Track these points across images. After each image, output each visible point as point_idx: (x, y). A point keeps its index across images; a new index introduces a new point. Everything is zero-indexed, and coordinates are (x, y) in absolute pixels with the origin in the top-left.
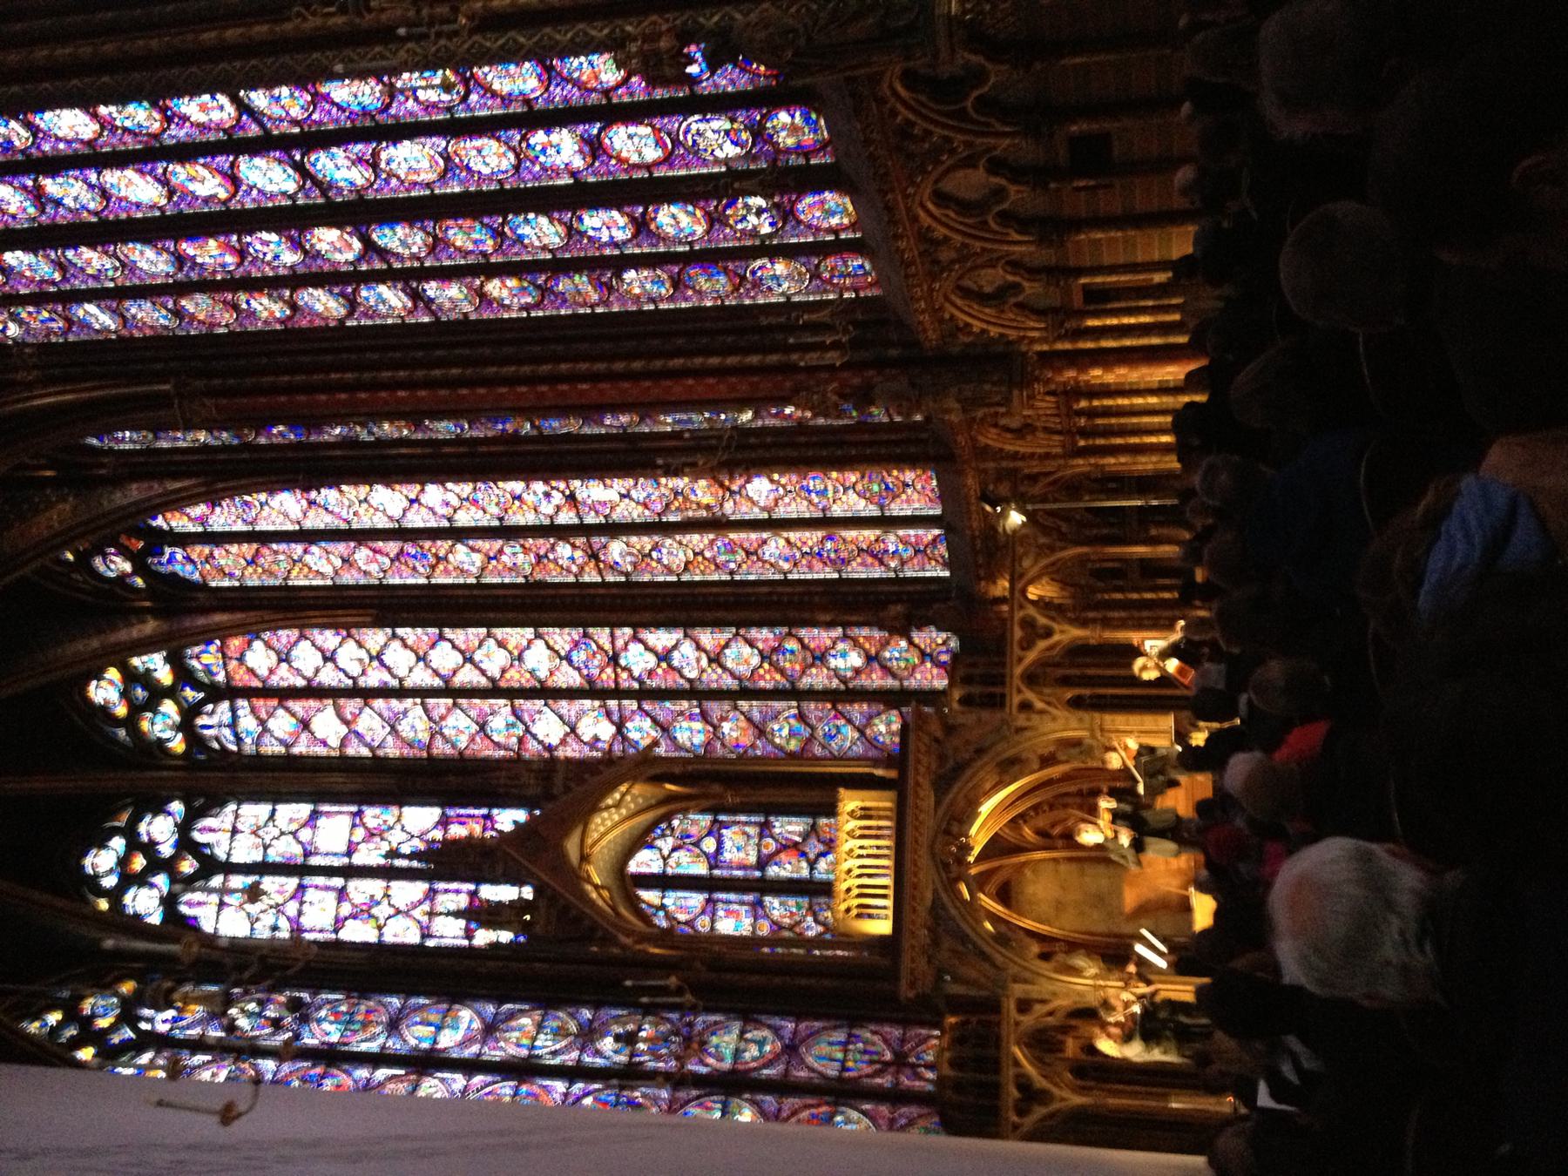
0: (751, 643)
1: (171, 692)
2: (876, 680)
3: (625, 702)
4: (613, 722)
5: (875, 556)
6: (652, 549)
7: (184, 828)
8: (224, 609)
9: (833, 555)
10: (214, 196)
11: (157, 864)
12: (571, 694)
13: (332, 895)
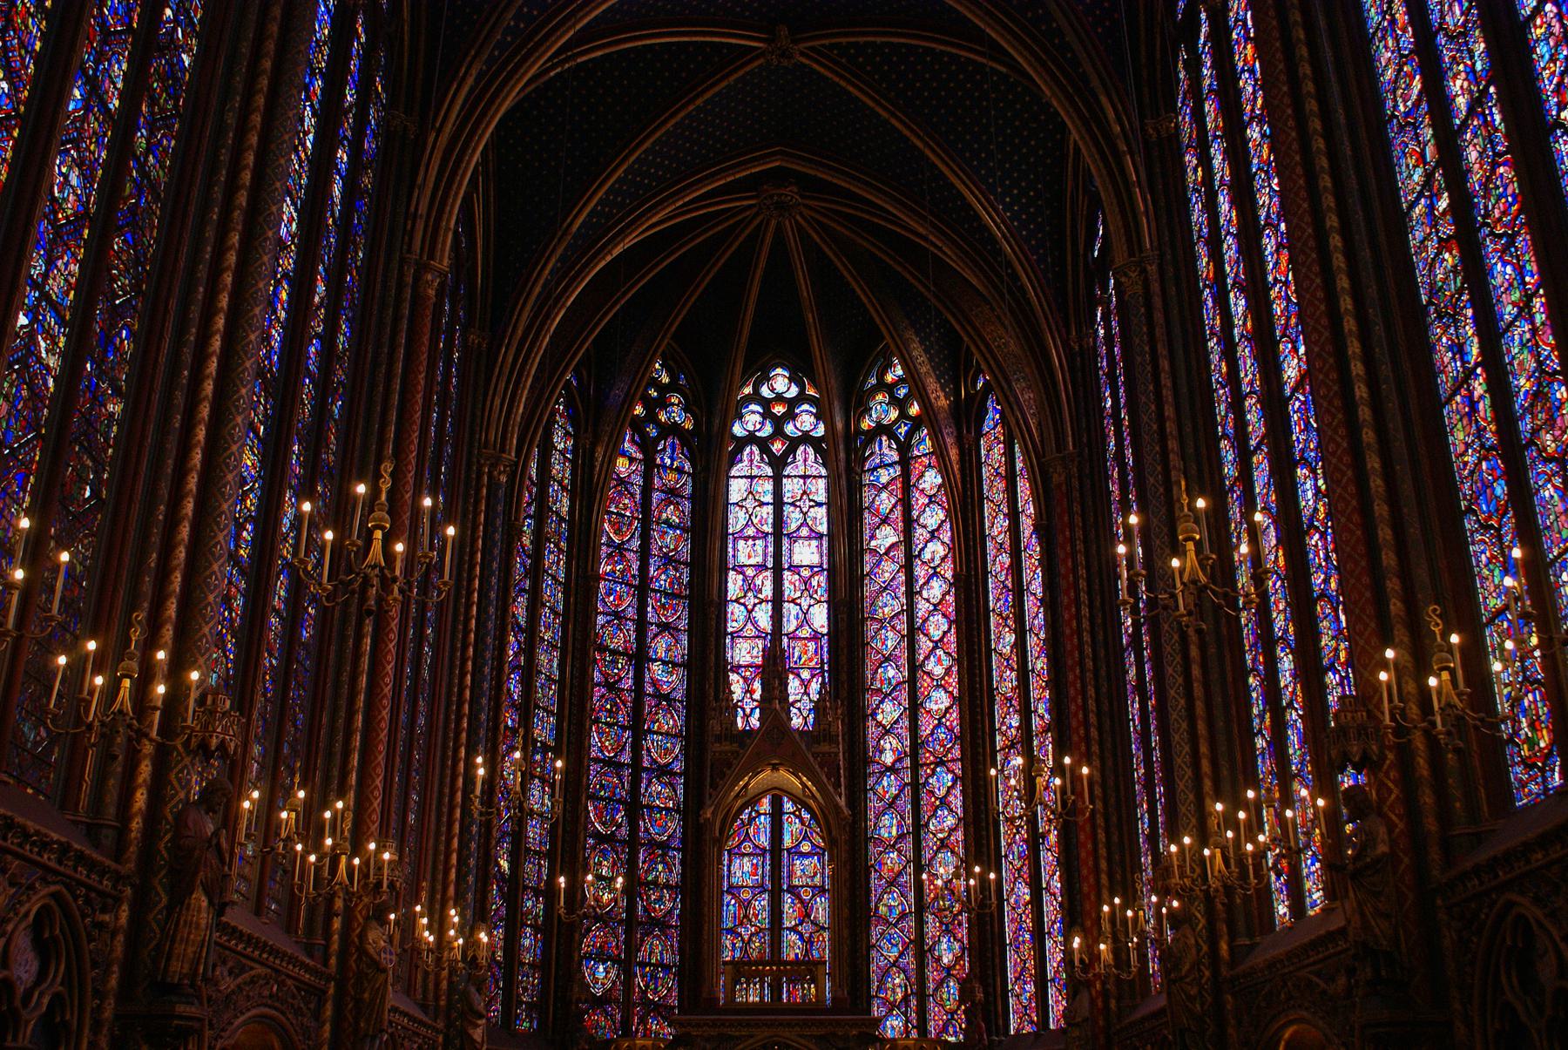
1: (903, 415)
2: (932, 975)
7: (806, 438)
8: (962, 454)
11: (779, 423)
12: (914, 728)
13: (759, 559)
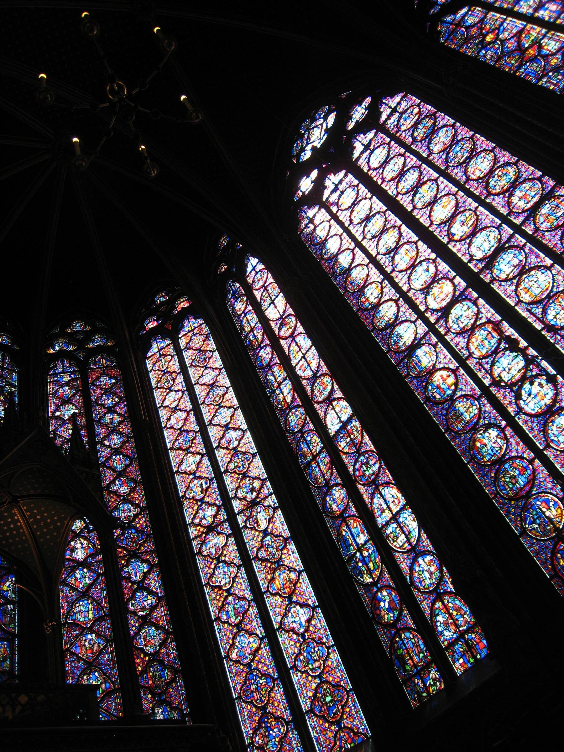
0: (163, 644)
3: (102, 566)
4: (85, 559)
5: (260, 721)
6: (225, 562)
9: (253, 687)
10: (453, 235)
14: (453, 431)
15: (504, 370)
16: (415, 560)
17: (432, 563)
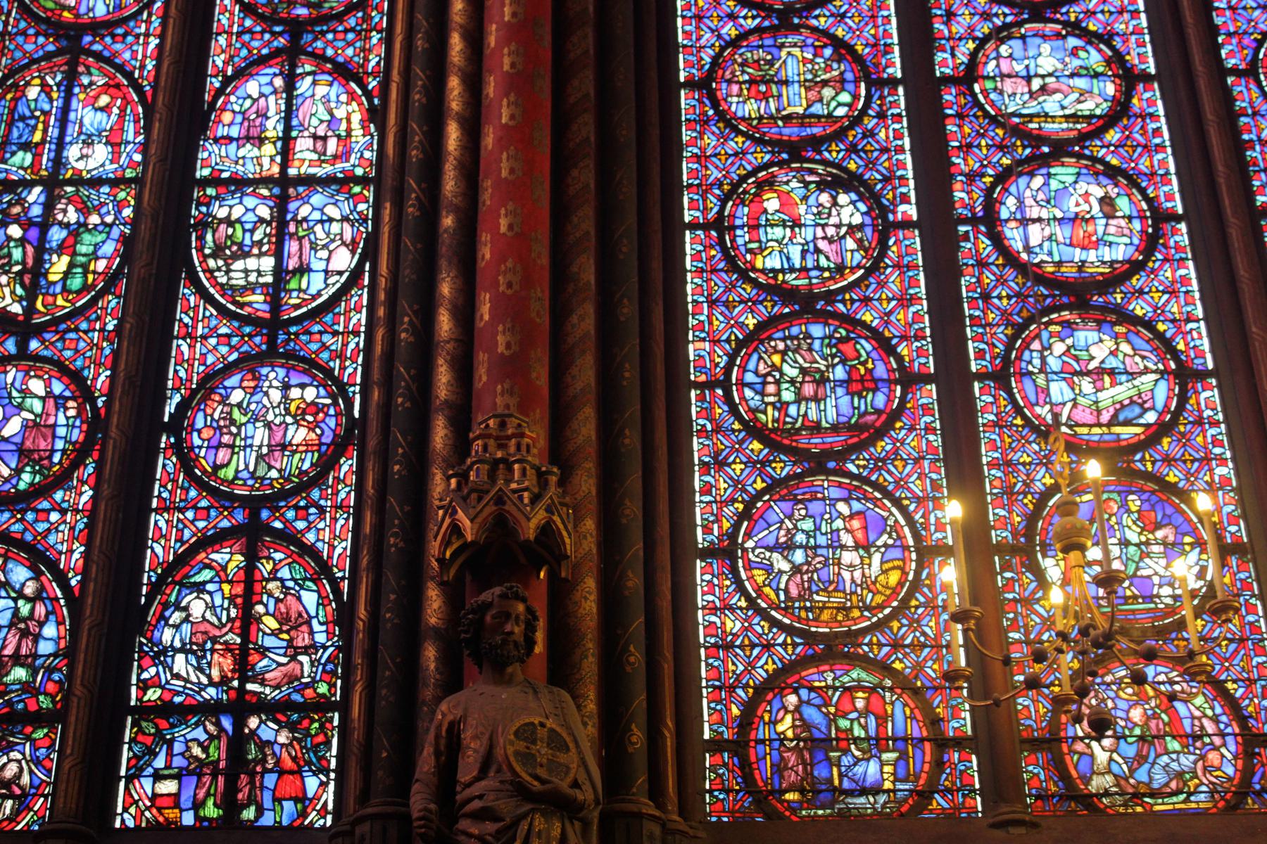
14: (715, 104)
15: (1028, 79)
16: (249, 364)
17: (310, 418)
